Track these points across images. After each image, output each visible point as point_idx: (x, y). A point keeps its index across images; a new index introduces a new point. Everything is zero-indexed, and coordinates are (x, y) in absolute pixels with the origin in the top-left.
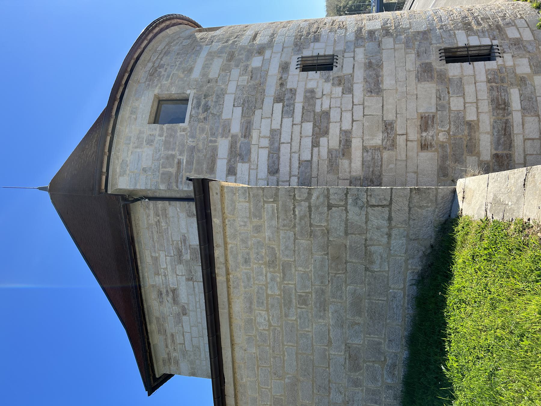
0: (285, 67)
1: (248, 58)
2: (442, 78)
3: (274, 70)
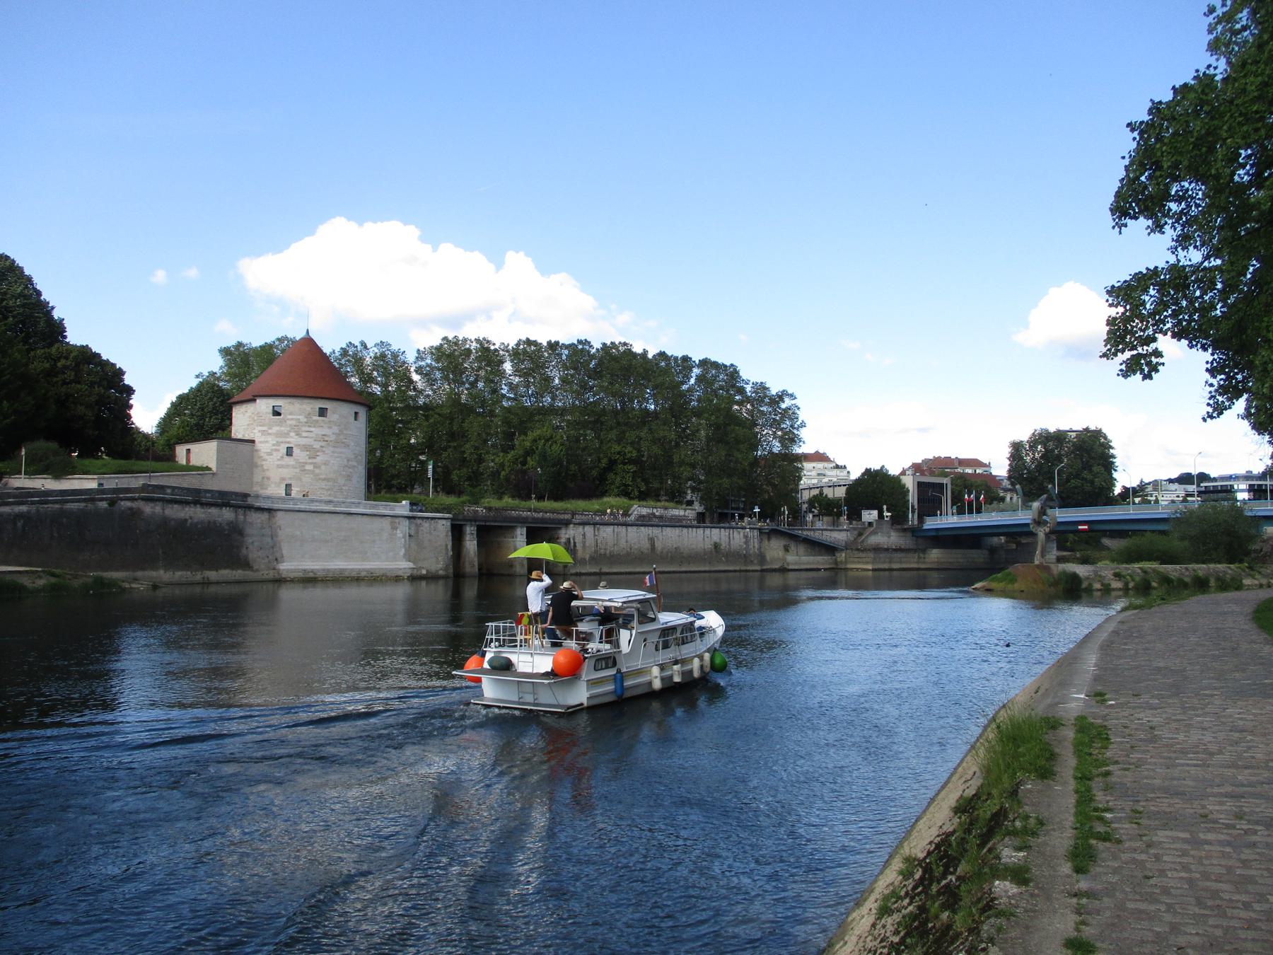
0: (289, 443)
1: (295, 432)
2: (280, 483)
3: (288, 440)
